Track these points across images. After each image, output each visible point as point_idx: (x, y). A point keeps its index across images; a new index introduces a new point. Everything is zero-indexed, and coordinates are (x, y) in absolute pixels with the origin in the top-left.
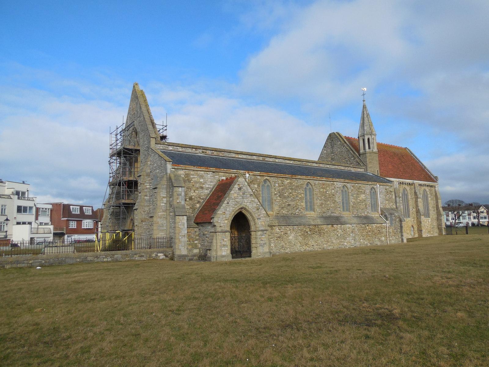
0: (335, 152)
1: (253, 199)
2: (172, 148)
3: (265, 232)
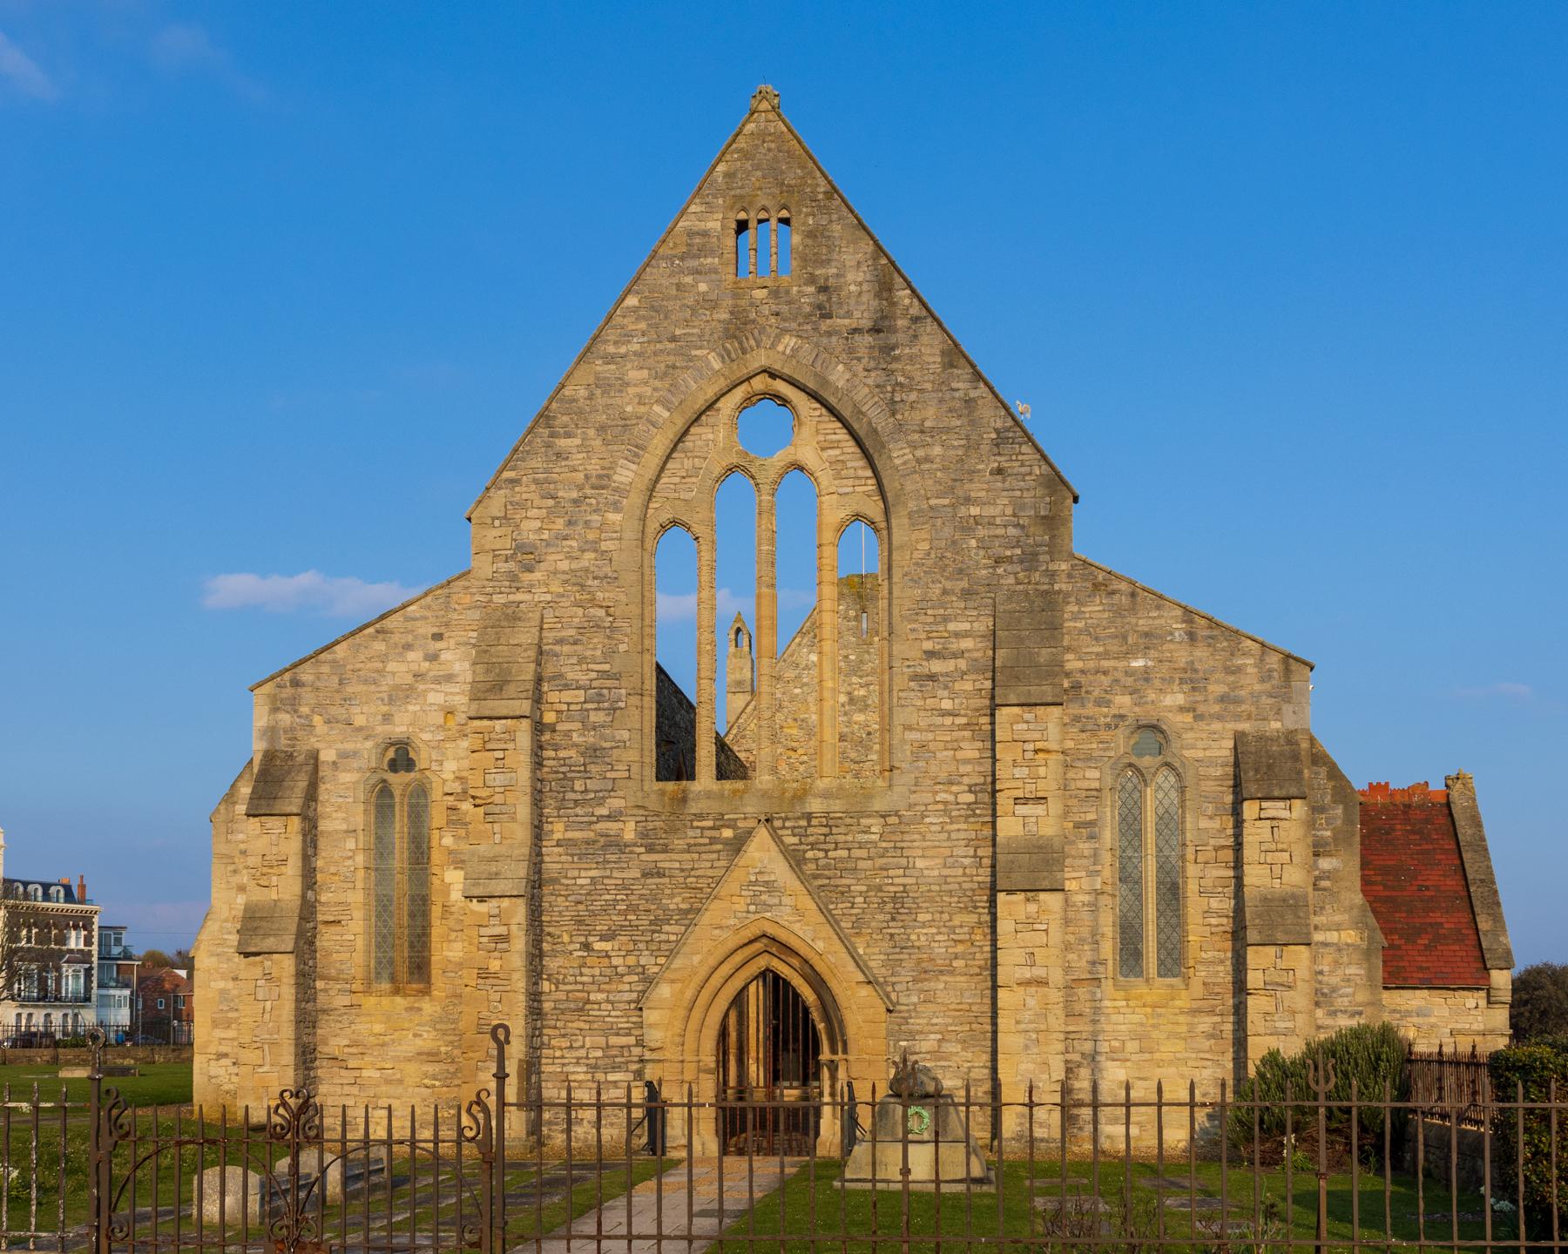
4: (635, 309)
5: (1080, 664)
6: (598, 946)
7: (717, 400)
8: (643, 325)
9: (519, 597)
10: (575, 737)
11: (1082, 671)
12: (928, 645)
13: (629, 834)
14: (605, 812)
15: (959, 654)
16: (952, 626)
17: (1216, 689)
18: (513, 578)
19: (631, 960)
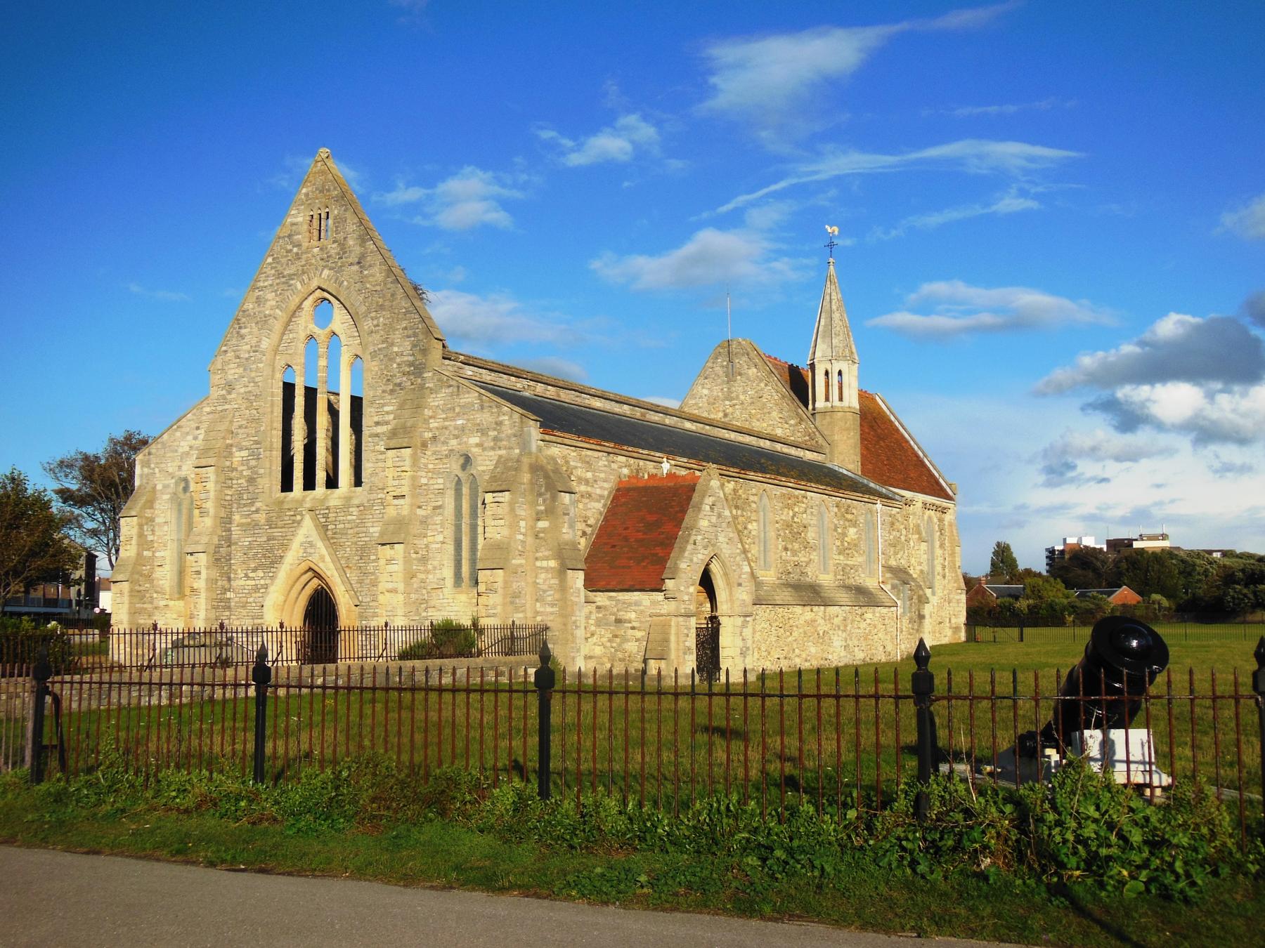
0: (737, 397)
1: (731, 535)
2: (470, 373)
3: (748, 619)
4: (270, 264)
5: (436, 425)
6: (251, 575)
7: (301, 304)
8: (273, 272)
9: (227, 407)
10: (245, 473)
11: (437, 428)
12: (376, 419)
13: (263, 521)
14: (254, 509)
15: (387, 423)
16: (387, 409)
17: (492, 433)
18: (224, 397)
19: (262, 582)
